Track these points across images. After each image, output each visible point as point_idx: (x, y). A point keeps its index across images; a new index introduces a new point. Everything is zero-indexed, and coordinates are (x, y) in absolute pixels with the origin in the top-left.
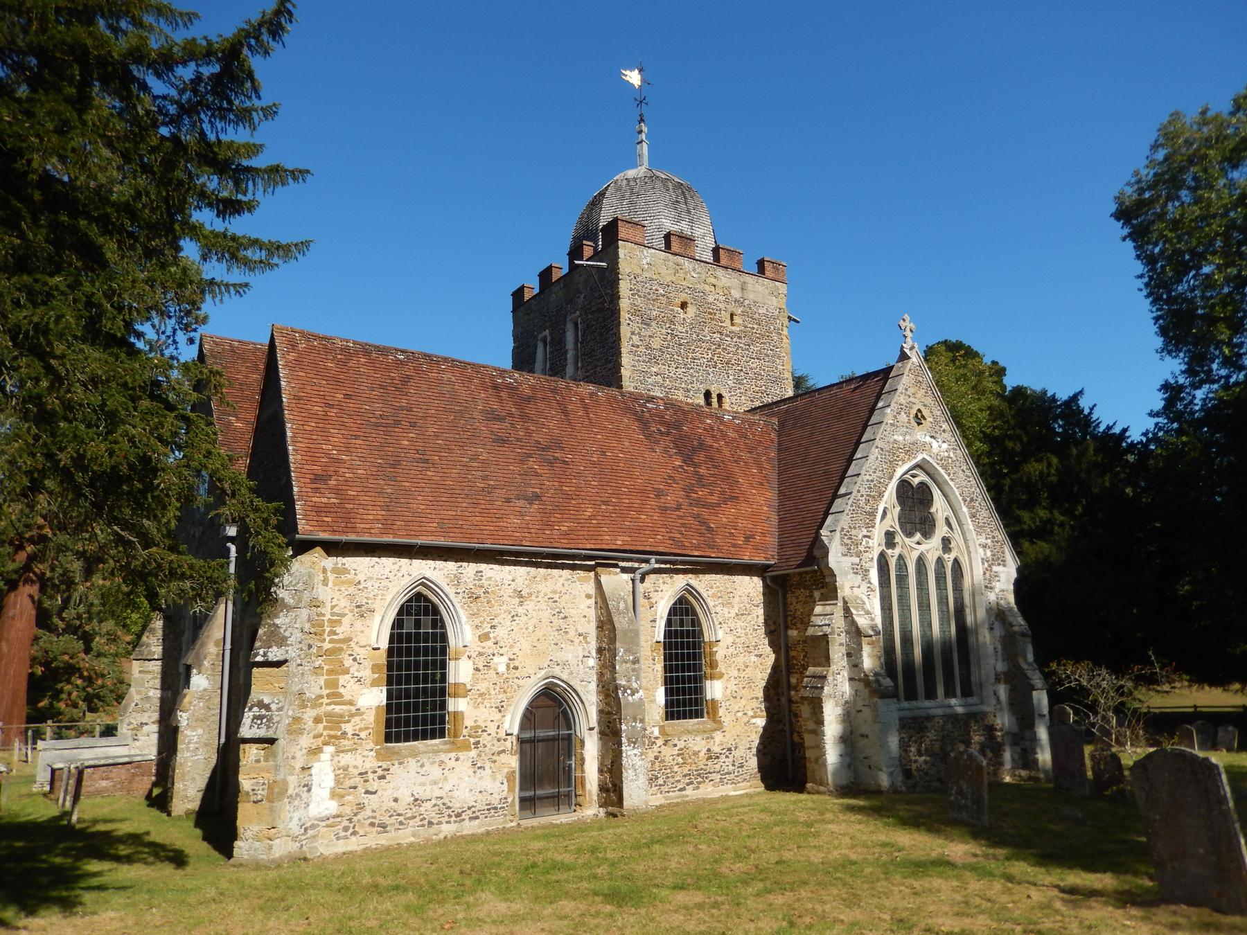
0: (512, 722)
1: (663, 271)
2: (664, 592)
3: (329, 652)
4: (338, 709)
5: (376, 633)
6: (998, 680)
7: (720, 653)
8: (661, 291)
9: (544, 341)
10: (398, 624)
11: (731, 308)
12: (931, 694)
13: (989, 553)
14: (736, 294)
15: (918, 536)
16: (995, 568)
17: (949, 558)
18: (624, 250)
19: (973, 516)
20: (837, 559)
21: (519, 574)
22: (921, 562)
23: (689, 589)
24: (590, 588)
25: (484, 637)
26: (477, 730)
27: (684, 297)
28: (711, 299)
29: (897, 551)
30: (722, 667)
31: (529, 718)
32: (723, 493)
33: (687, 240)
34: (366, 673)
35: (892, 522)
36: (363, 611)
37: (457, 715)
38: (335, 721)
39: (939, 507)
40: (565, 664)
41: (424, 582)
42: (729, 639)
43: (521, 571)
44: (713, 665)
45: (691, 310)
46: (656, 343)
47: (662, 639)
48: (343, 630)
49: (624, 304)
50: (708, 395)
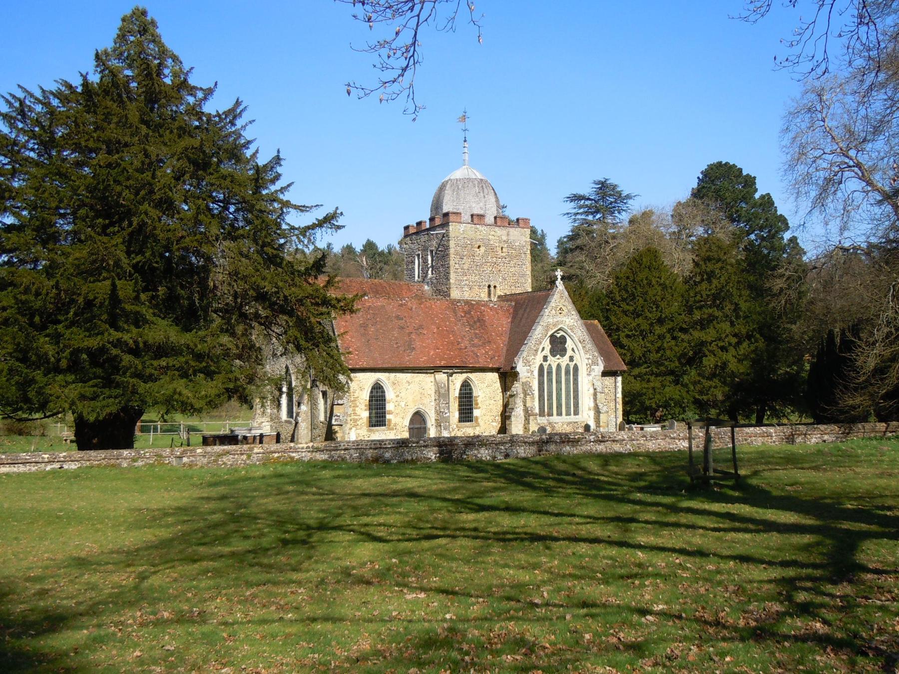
0: (407, 422)
1: (470, 233)
2: (458, 380)
5: (365, 396)
6: (590, 409)
7: (479, 400)
9: (418, 255)
10: (371, 392)
11: (501, 245)
14: (504, 238)
15: (558, 356)
17: (572, 365)
18: (452, 227)
19: (584, 347)
20: (520, 368)
21: (408, 376)
22: (559, 366)
23: (468, 378)
24: (433, 379)
25: (398, 396)
26: (395, 425)
27: (479, 243)
28: (492, 242)
30: (480, 405)
31: (412, 421)
33: (481, 217)
34: (363, 407)
35: (547, 352)
36: (361, 389)
37: (390, 420)
38: (355, 421)
39: (569, 344)
40: (423, 404)
43: (409, 375)
44: (477, 404)
45: (482, 249)
46: (466, 267)
48: (356, 395)
49: (452, 251)
50: (489, 286)
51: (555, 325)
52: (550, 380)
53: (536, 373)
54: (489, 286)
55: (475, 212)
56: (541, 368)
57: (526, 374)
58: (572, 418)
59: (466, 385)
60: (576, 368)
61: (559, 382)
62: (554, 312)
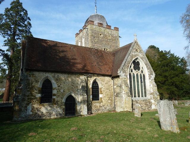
0: (64, 100)
3: (31, 88)
4: (32, 97)
5: (39, 85)
10: (43, 84)
13: (150, 73)
14: (110, 33)
16: (151, 76)
25: (59, 86)
30: (102, 92)
32: (104, 63)
36: (37, 82)
37: (54, 99)
41: (47, 77)
42: (104, 88)
45: (102, 35)
46: (96, 41)
48: (33, 84)
50: (105, 49)
51: (135, 56)
52: (134, 81)
56: (130, 74)
57: (124, 77)
58: (144, 98)
59: (95, 82)
60: (144, 76)
61: (138, 81)
62: (134, 50)
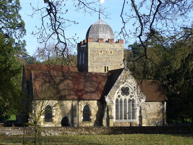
8: (96, 50)
12: (121, 119)
14: (112, 48)
22: (125, 99)
27: (101, 50)
28: (106, 49)
29: (120, 98)
30: (92, 114)
44: (91, 114)
45: (102, 52)
46: (95, 59)
47: (83, 110)
49: (89, 53)
50: (105, 67)
52: (121, 105)
53: (114, 102)
54: (105, 67)
55: (100, 37)
56: (117, 100)
57: (109, 102)
